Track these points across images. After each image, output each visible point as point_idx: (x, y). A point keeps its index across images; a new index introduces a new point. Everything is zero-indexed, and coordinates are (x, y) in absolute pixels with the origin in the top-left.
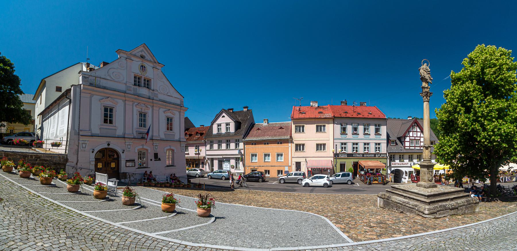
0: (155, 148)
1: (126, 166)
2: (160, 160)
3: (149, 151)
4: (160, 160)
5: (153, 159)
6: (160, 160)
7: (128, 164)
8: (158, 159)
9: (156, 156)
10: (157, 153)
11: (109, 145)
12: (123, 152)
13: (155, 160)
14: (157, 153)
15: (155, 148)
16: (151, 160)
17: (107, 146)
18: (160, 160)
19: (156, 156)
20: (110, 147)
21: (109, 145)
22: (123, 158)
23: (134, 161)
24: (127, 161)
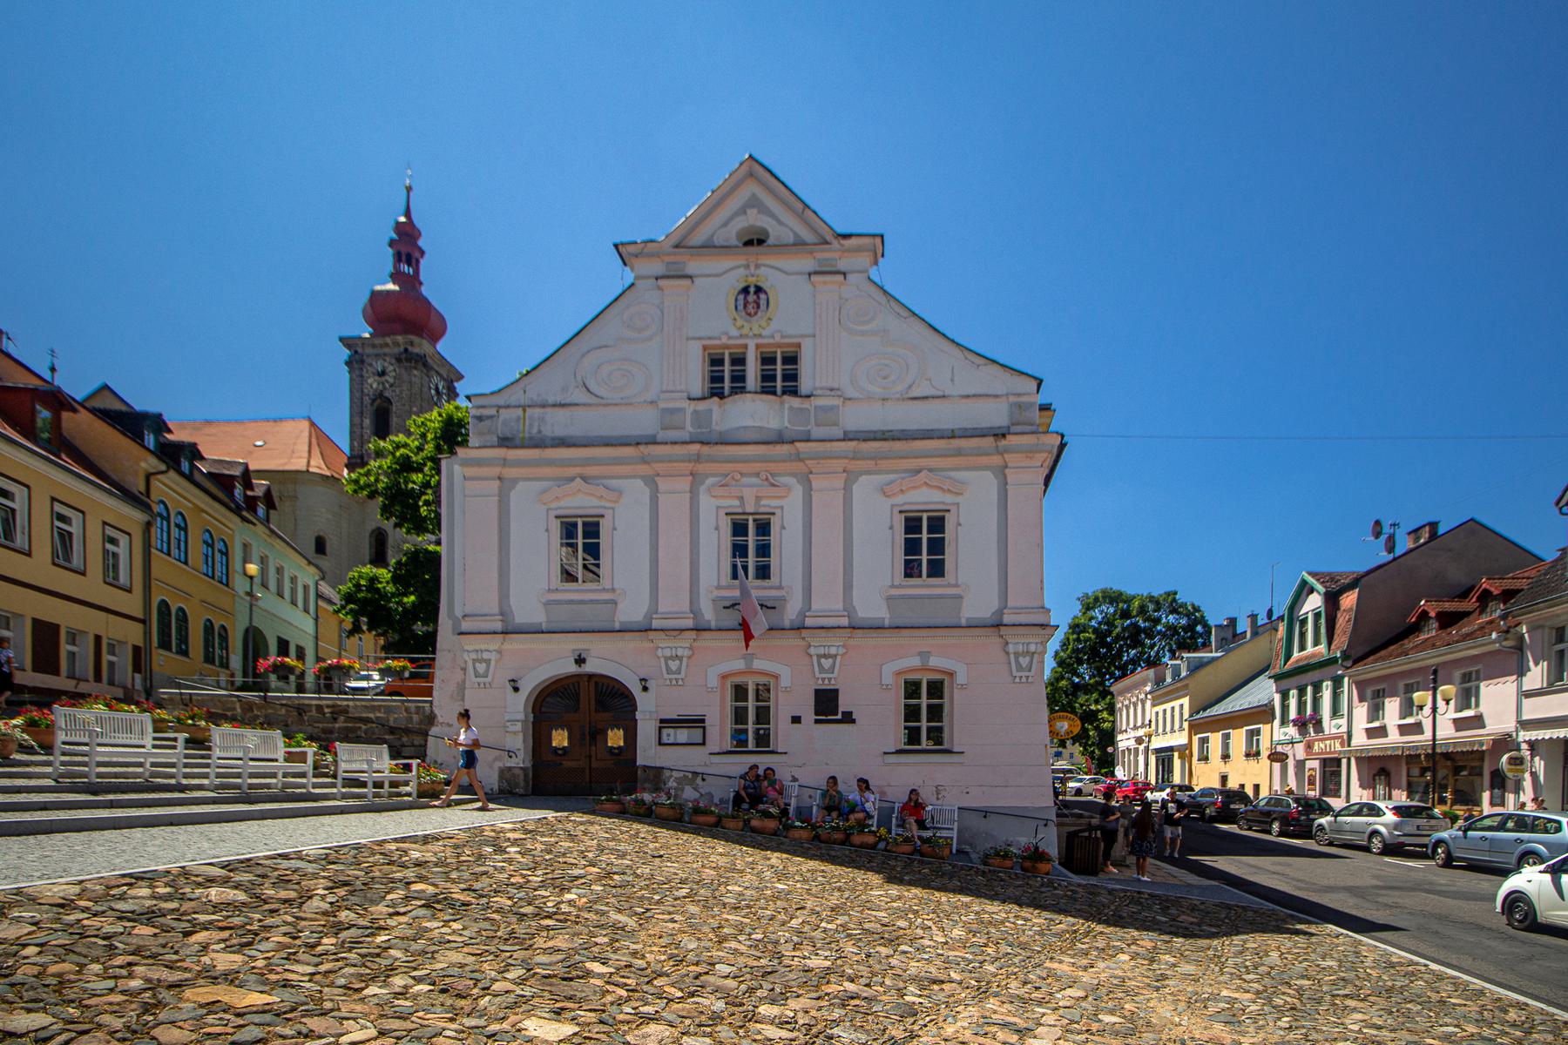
0: (820, 665)
1: (660, 743)
2: (848, 718)
3: (785, 681)
4: (853, 721)
5: (809, 715)
6: (848, 718)
7: (670, 735)
8: (839, 717)
9: (827, 704)
10: (836, 691)
11: (580, 661)
12: (645, 689)
13: (817, 721)
14: (836, 691)
15: (820, 665)
16: (796, 720)
17: (572, 668)
18: (853, 721)
19: (827, 704)
20: (589, 668)
21: (580, 661)
22: (648, 709)
23: (703, 721)
24: (665, 723)
